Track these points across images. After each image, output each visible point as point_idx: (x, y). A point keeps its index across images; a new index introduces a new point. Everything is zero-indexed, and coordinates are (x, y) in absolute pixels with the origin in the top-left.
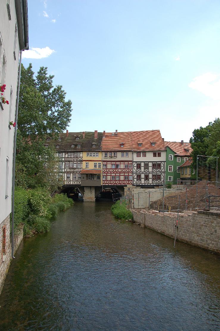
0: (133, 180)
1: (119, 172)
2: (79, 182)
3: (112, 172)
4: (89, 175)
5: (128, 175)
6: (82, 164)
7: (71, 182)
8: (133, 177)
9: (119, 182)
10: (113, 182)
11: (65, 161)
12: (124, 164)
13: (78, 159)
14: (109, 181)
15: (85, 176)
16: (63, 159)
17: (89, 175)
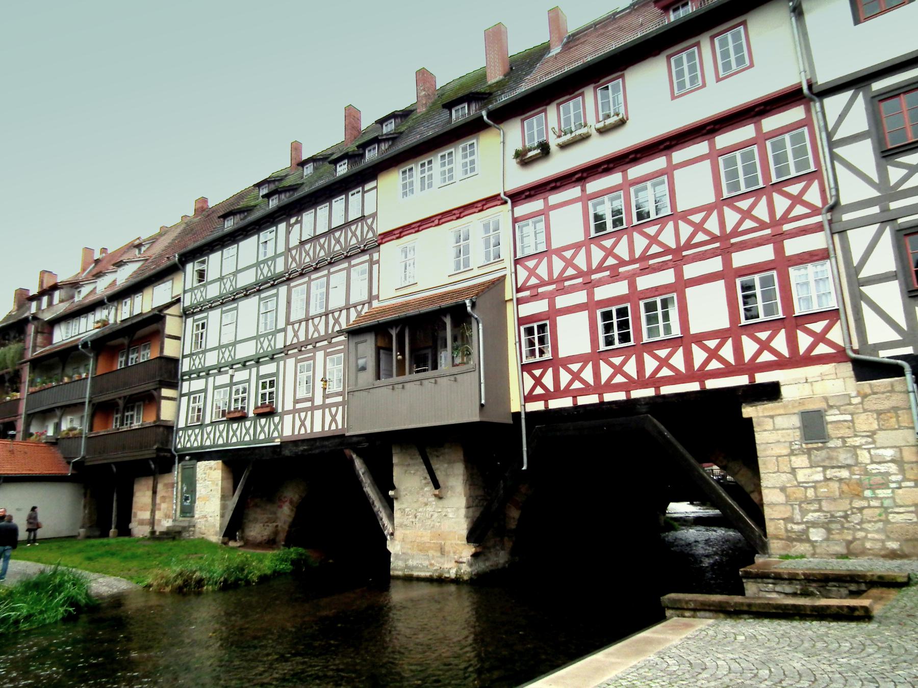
0: (858, 298)
1: (667, 251)
2: (334, 410)
3: (600, 269)
4: (394, 333)
5: (783, 263)
6: (375, 267)
7: (318, 414)
8: (853, 272)
9: (678, 360)
10: (618, 370)
11: (287, 278)
12: (714, 155)
13: (354, 234)
14: (575, 367)
15: (368, 347)
16: (280, 267)
17: (394, 333)
